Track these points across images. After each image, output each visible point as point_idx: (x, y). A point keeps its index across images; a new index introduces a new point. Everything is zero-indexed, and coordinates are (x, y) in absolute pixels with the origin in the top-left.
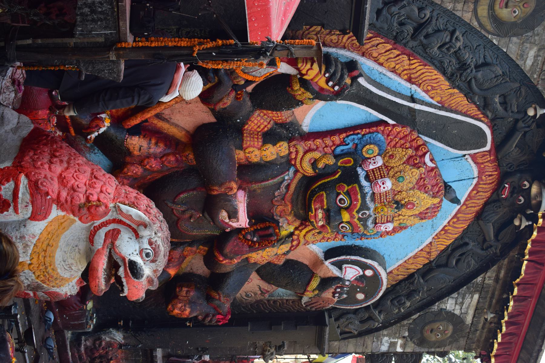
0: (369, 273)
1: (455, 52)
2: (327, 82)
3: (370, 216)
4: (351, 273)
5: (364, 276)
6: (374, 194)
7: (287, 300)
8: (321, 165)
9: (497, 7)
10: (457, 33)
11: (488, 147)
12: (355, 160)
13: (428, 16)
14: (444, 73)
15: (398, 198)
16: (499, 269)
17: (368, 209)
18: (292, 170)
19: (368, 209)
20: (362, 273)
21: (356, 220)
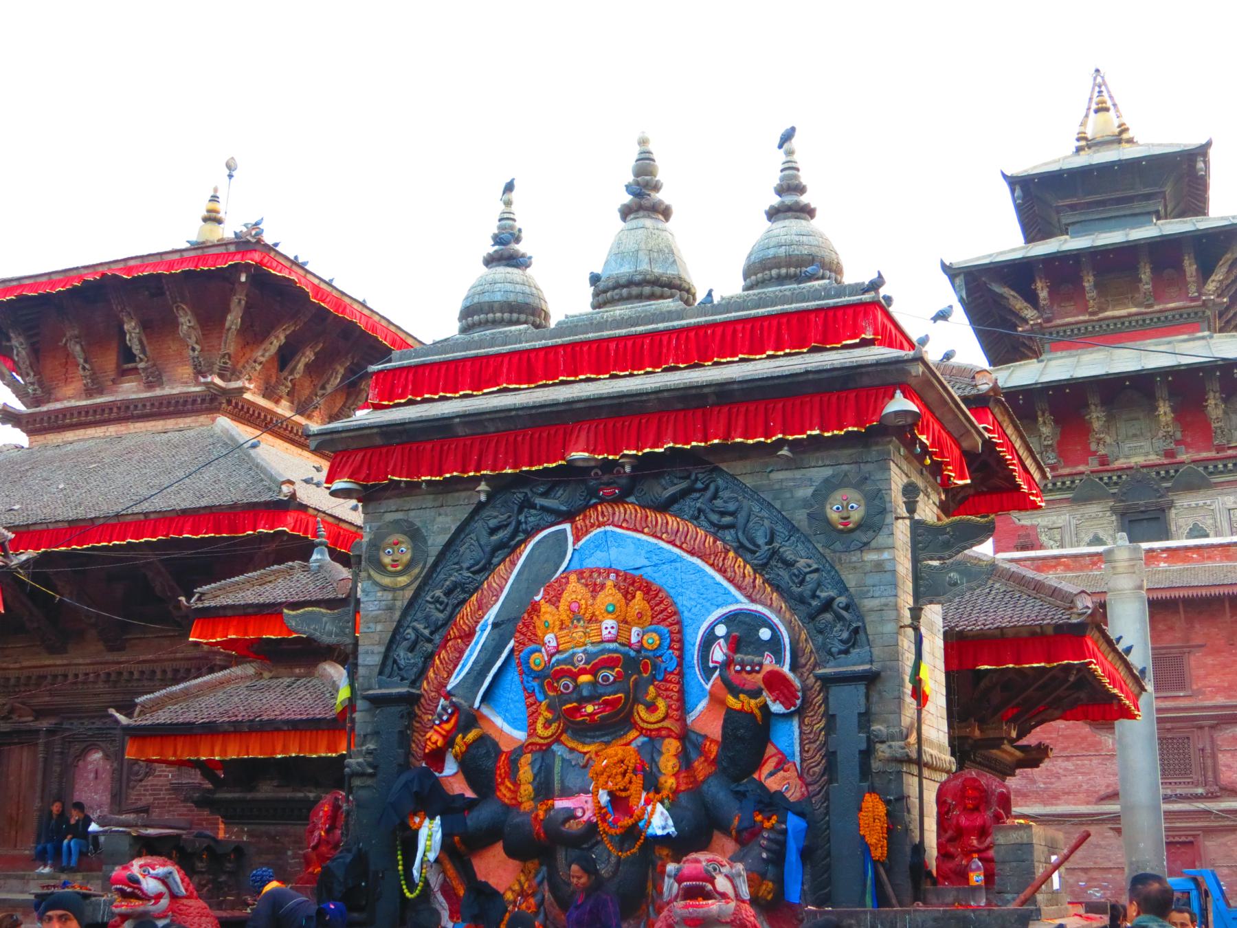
0: (721, 630)
1: (445, 594)
2: (448, 721)
3: (584, 652)
4: (718, 654)
5: (726, 637)
6: (558, 652)
7: (801, 733)
8: (550, 716)
9: (399, 568)
10: (428, 598)
11: (567, 526)
12: (546, 677)
13: (409, 631)
14: (464, 601)
15: (567, 622)
16: (724, 461)
17: (574, 654)
18: (555, 747)
19: (574, 654)
20: (722, 641)
21: (588, 667)
